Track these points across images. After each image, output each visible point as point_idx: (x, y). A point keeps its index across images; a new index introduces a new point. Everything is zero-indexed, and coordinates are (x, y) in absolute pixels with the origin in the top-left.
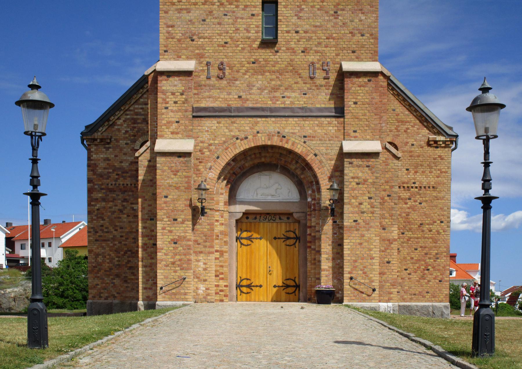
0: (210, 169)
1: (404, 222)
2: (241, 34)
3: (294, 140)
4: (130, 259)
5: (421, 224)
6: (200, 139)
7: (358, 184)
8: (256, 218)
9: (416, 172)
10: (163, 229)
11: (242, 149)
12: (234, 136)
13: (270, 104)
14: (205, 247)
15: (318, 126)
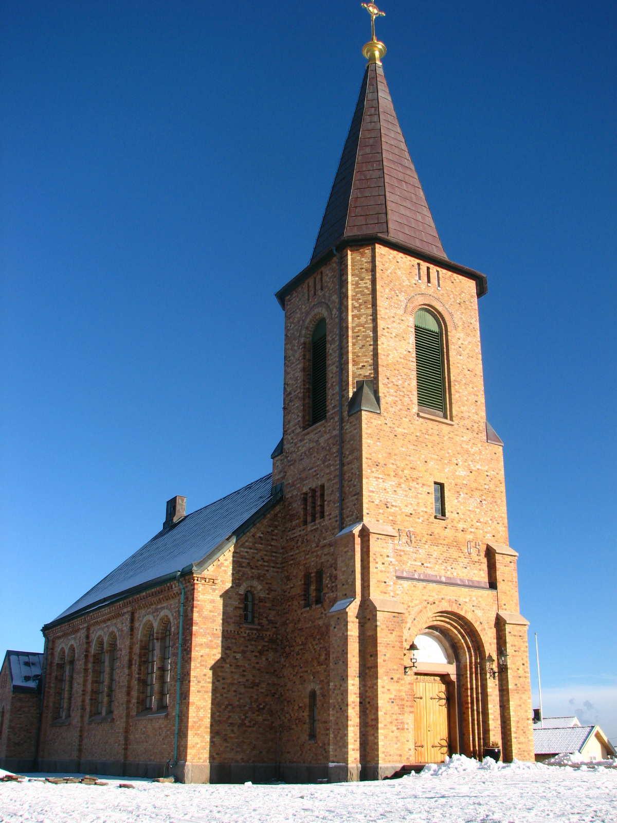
4: (230, 714)
7: (515, 651)
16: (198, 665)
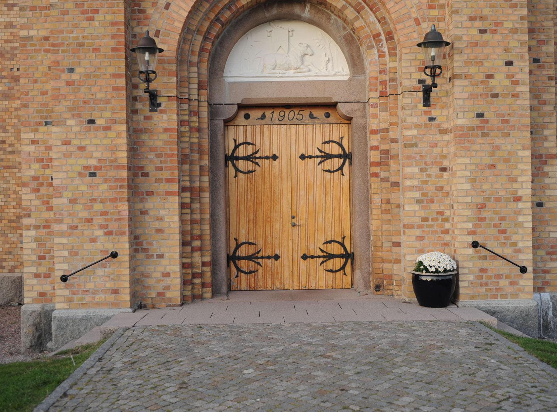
7: (483, 32)
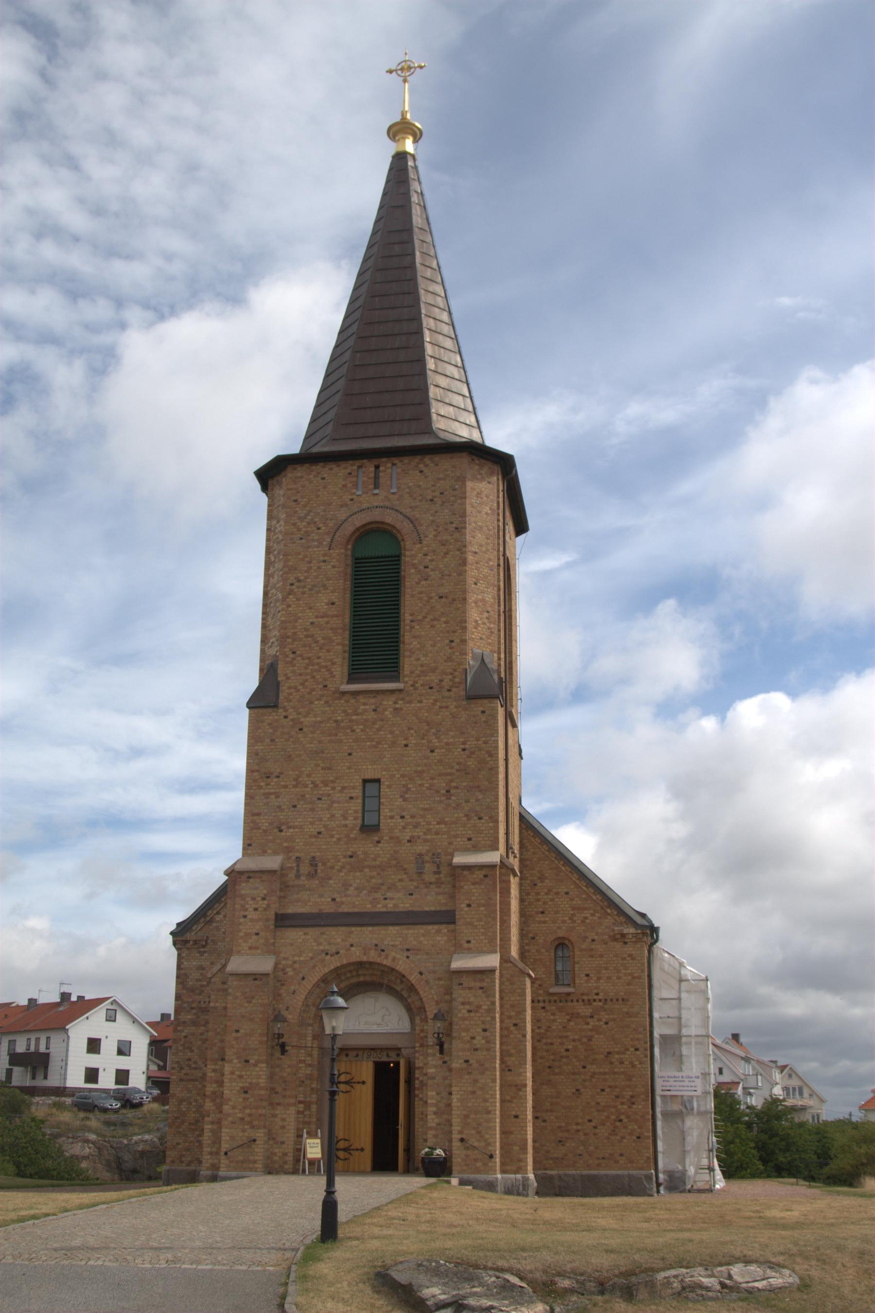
0: (294, 992)
1: (586, 1050)
2: (337, 822)
3: (393, 954)
5: (609, 1053)
6: (282, 955)
7: (469, 1011)
8: (357, 1055)
9: (599, 978)
10: (232, 1073)
11: (332, 968)
12: (323, 951)
13: (369, 908)
14: (284, 1097)
15: (423, 935)
16: (181, 1048)
